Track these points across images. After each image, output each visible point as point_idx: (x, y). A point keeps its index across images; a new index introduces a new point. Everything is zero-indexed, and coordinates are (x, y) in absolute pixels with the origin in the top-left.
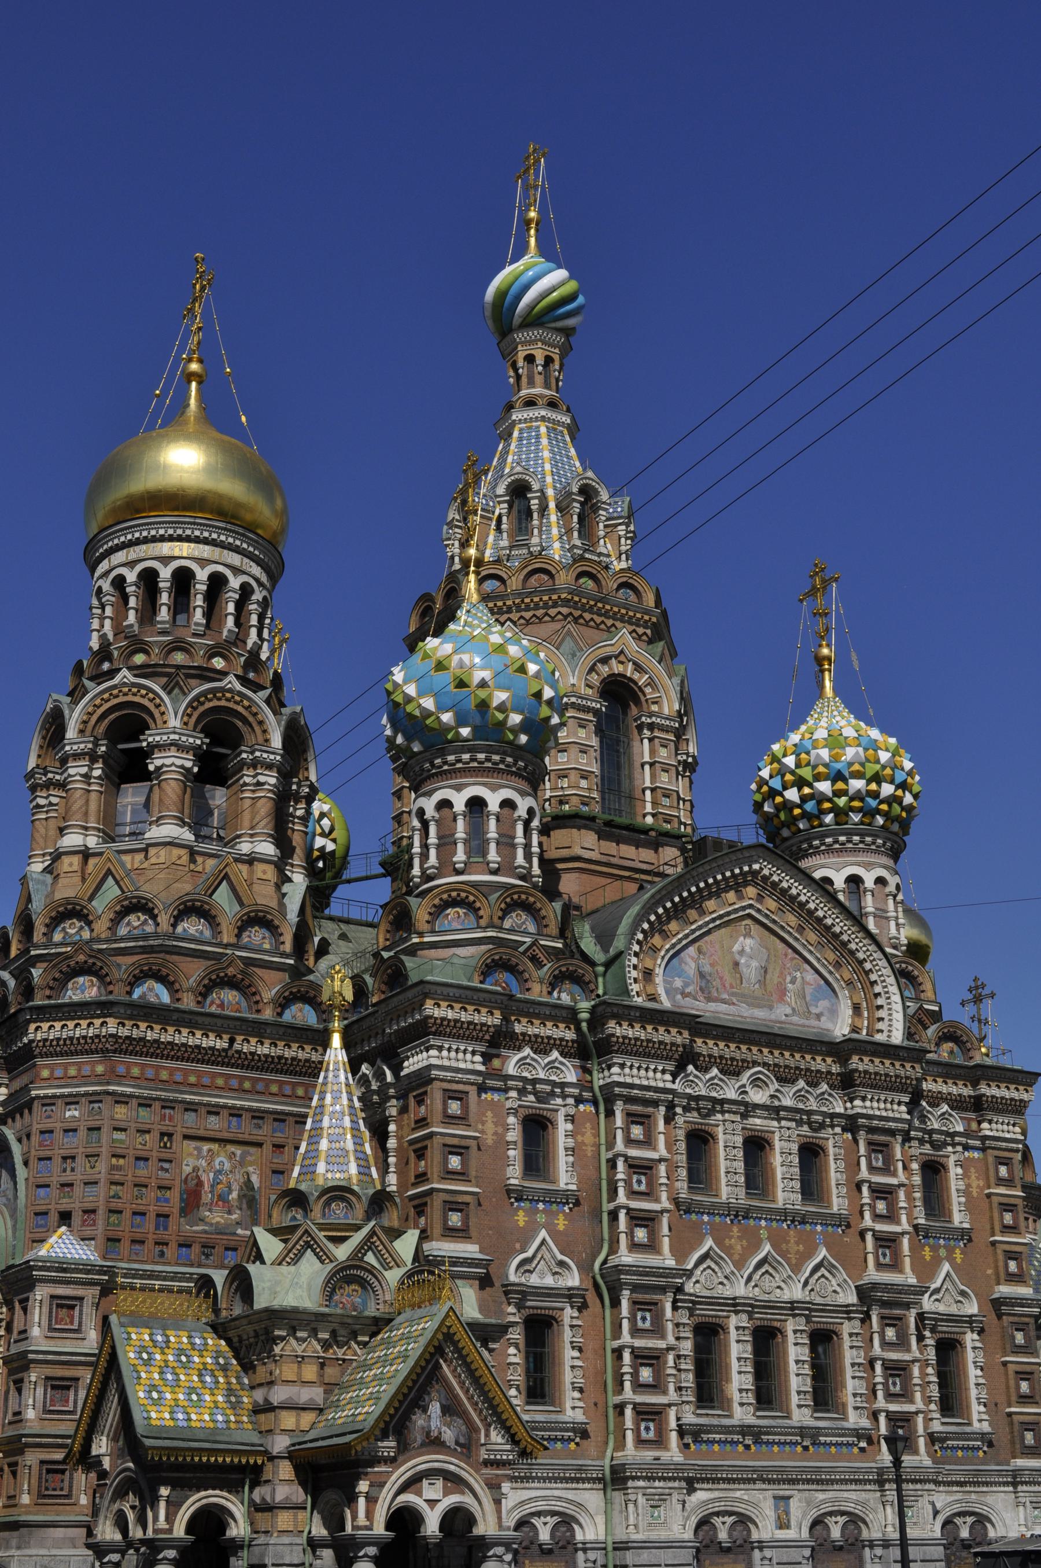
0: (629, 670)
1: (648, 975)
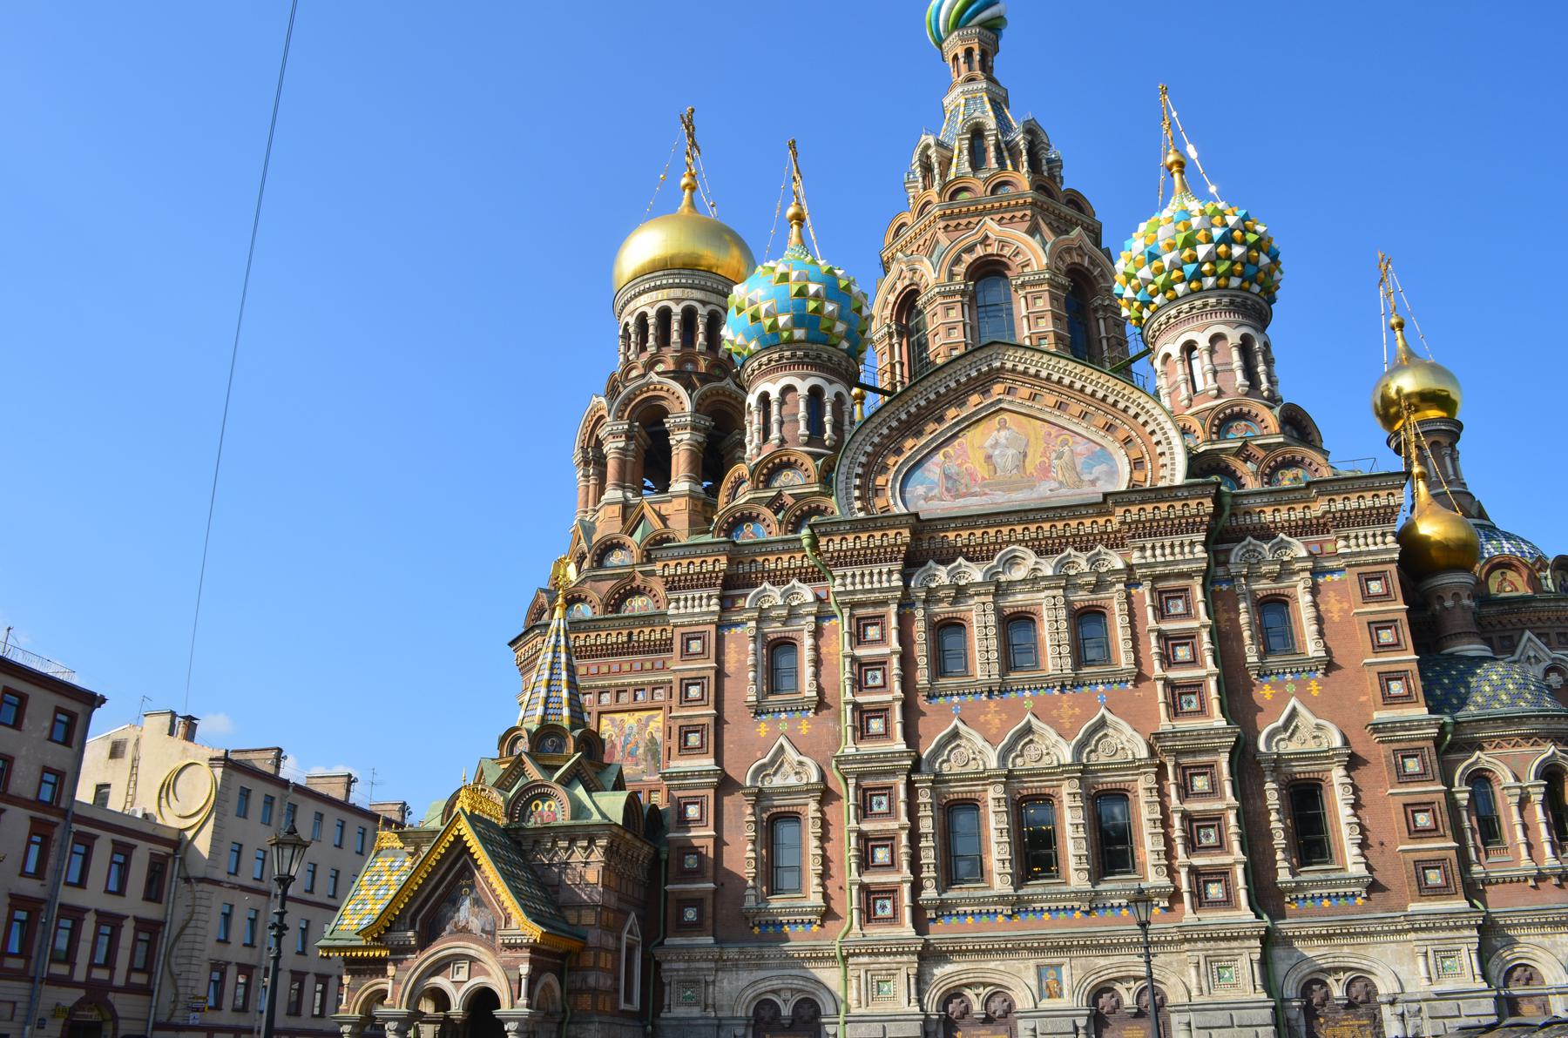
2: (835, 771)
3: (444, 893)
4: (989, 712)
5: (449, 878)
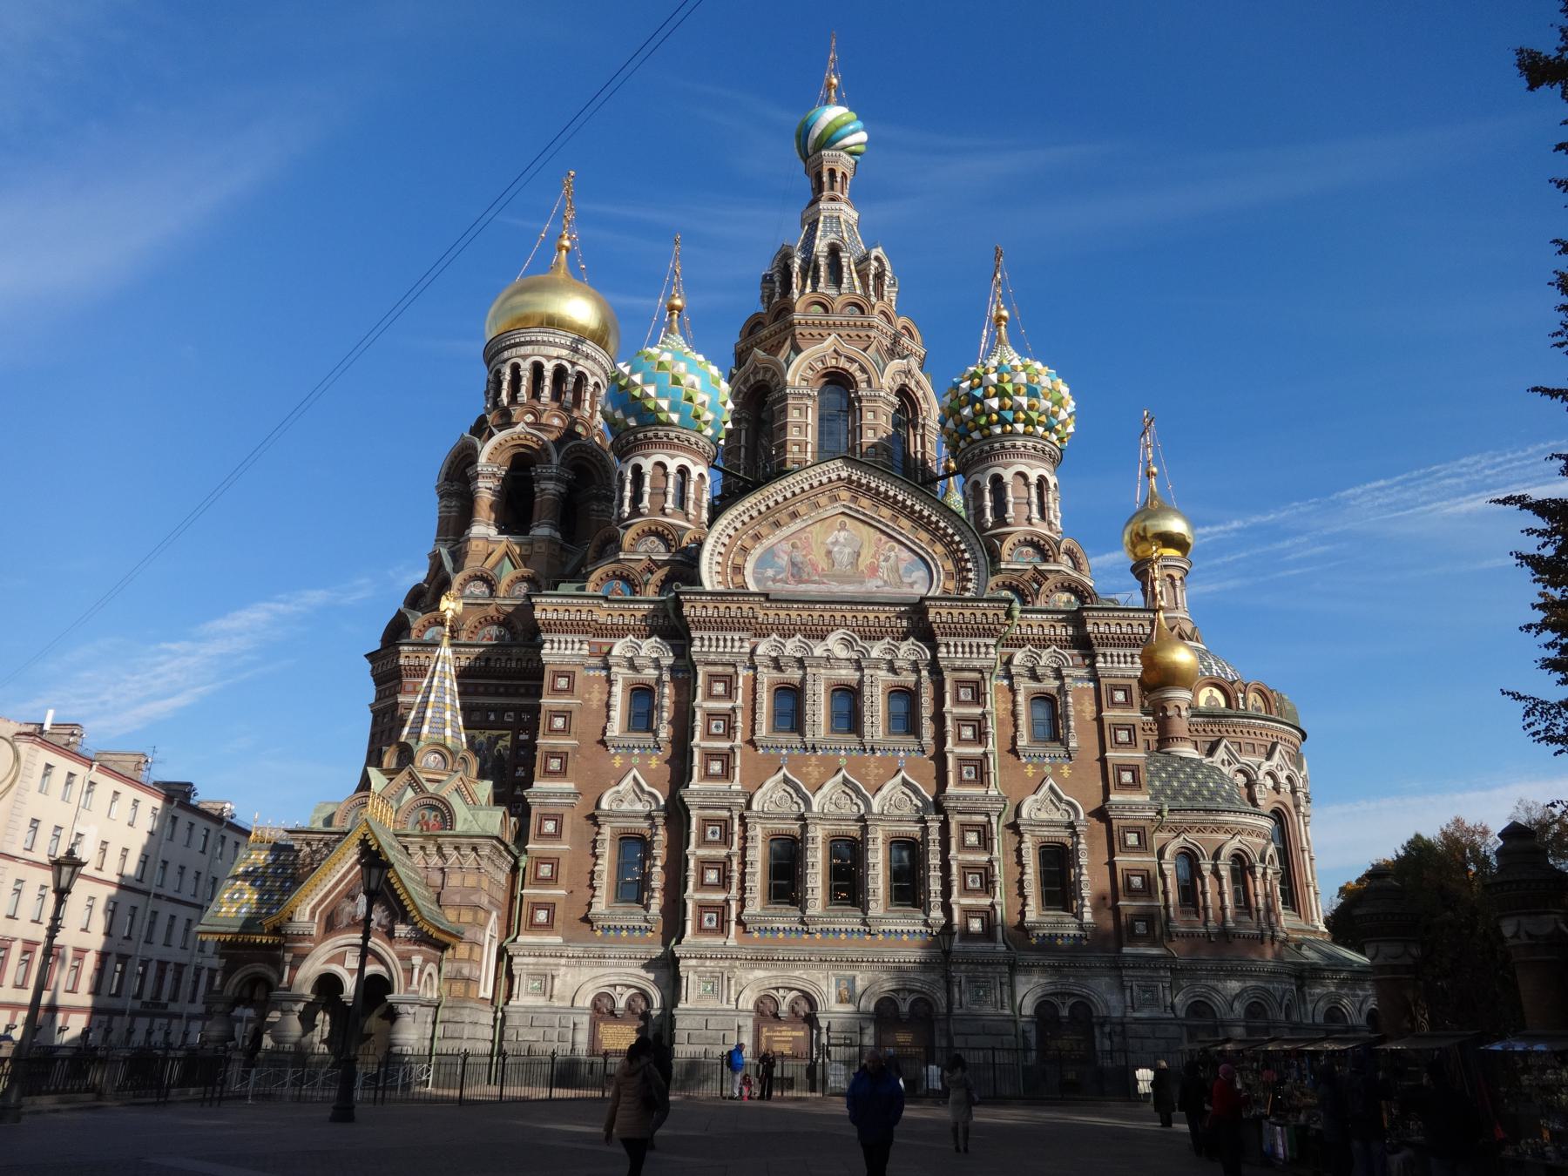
0: (843, 363)
1: (738, 569)
2: (678, 802)
3: (344, 889)
4: (808, 766)
5: (349, 877)
